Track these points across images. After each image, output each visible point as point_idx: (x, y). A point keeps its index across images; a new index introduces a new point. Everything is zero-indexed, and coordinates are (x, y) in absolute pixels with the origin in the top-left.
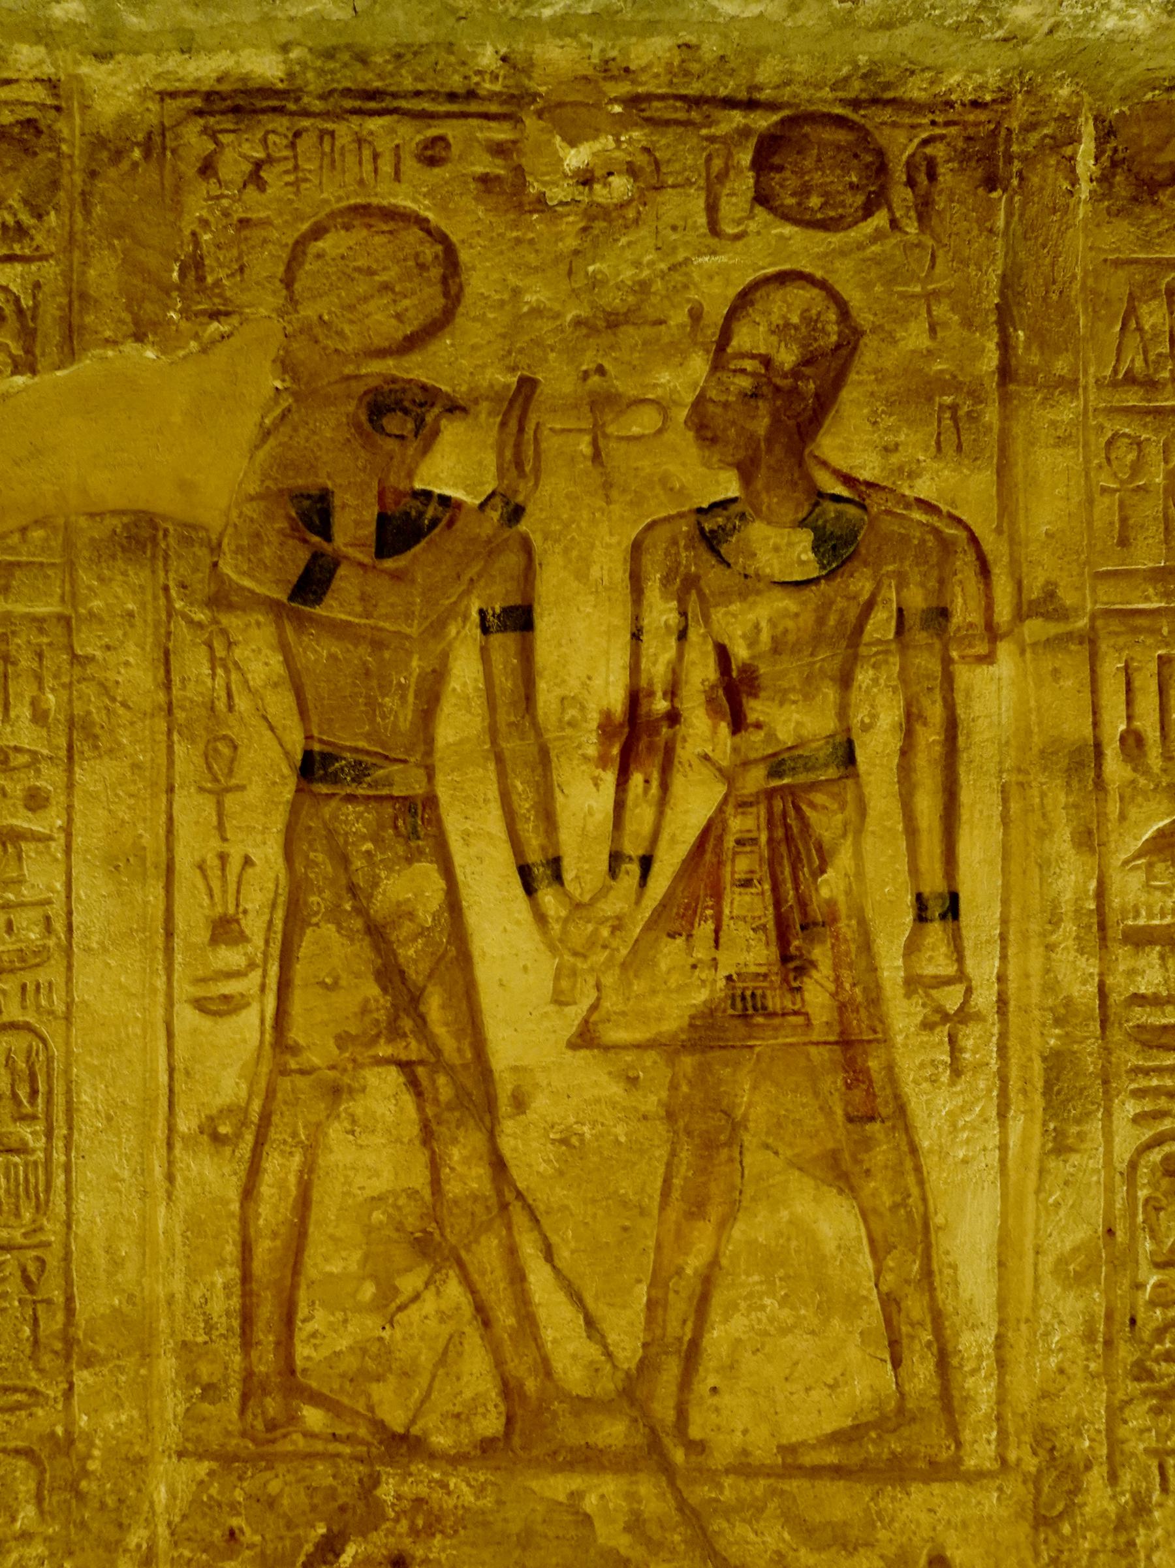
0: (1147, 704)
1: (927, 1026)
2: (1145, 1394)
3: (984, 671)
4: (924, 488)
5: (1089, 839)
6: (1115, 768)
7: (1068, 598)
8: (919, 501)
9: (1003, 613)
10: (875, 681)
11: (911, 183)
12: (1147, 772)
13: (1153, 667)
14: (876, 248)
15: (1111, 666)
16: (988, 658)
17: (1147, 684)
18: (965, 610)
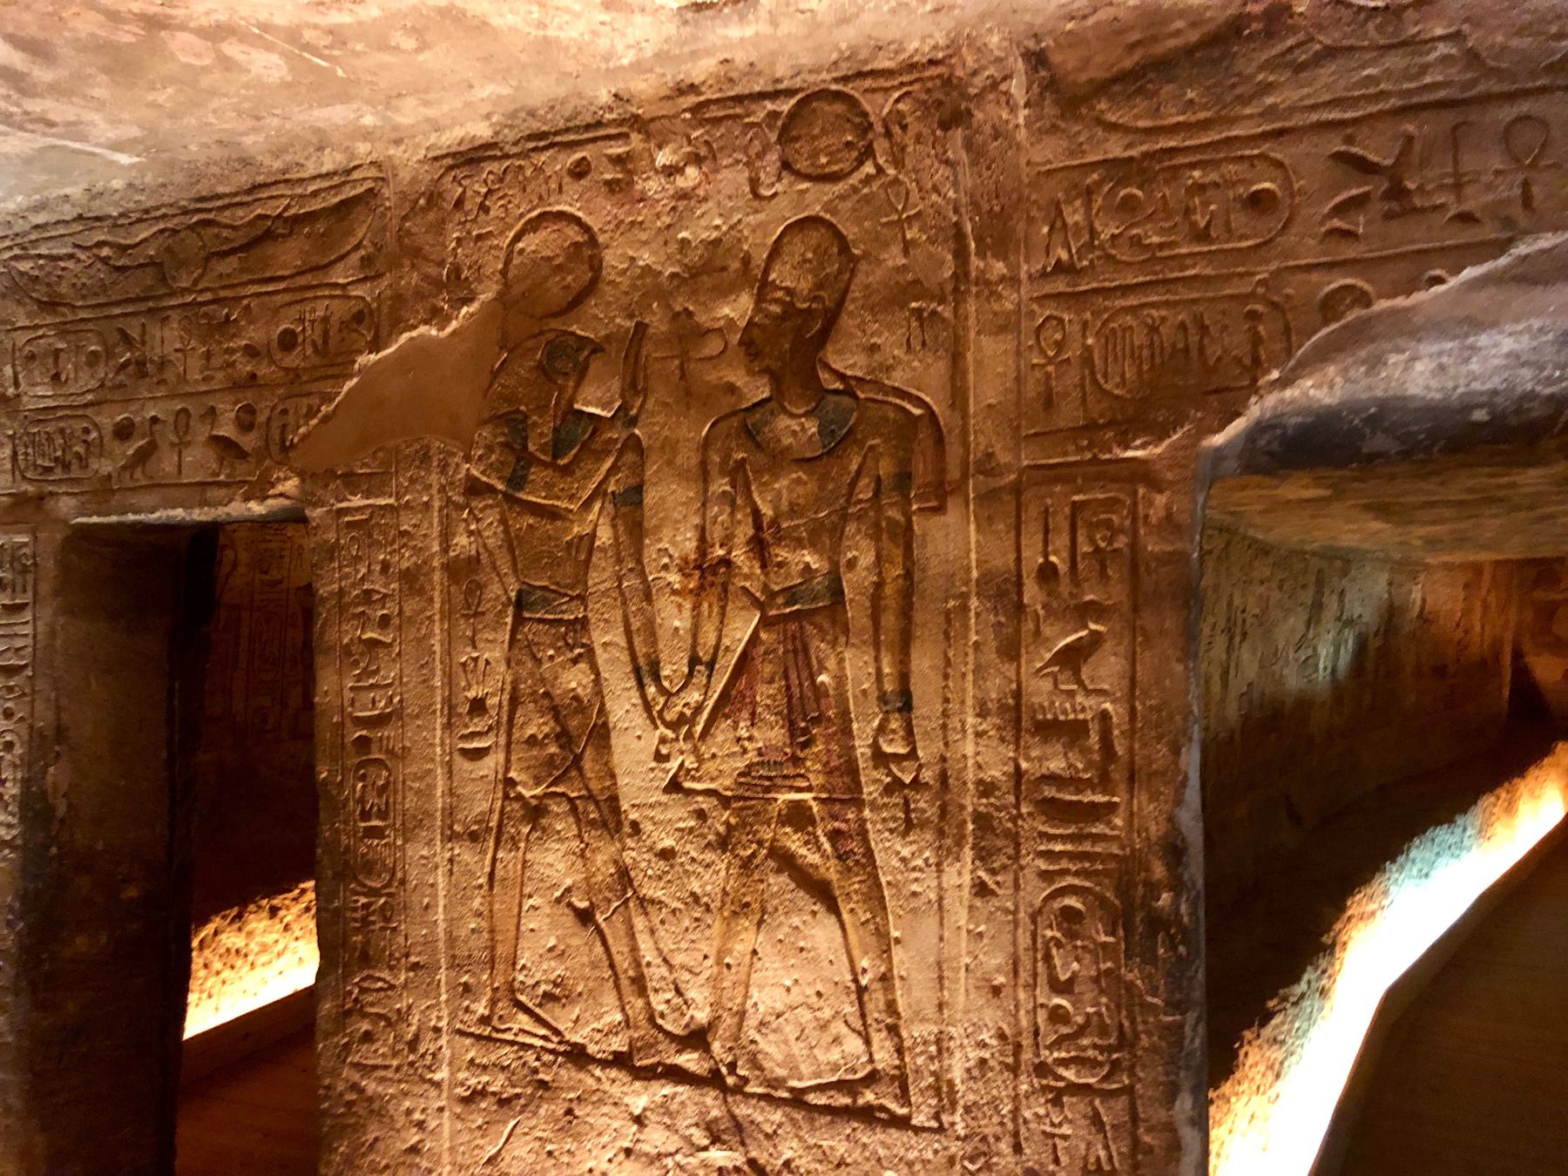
0: (1061, 541)
1: (888, 790)
2: (1045, 1089)
3: (938, 520)
4: (898, 379)
5: (1011, 651)
6: (1032, 593)
7: (1004, 457)
8: (894, 388)
9: (954, 474)
10: (859, 531)
11: (888, 134)
12: (1058, 596)
13: (1067, 510)
14: (866, 190)
15: (1032, 512)
16: (940, 509)
17: (1061, 521)
18: (921, 469)
